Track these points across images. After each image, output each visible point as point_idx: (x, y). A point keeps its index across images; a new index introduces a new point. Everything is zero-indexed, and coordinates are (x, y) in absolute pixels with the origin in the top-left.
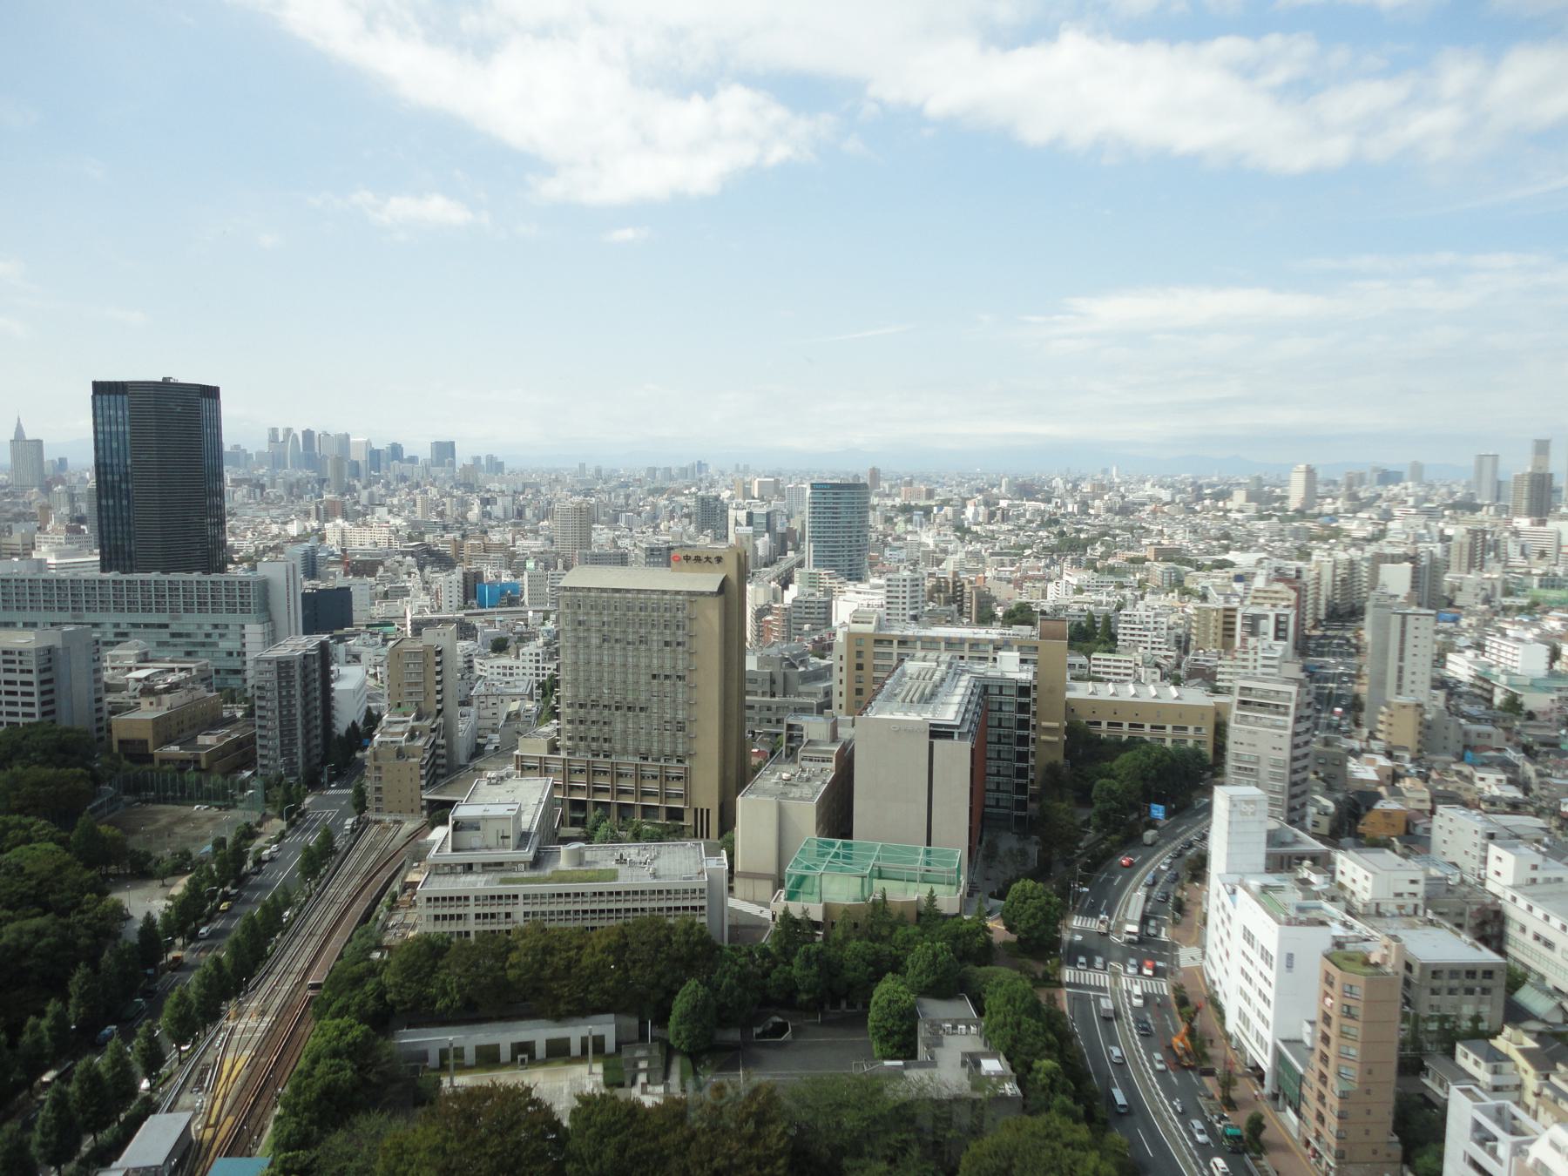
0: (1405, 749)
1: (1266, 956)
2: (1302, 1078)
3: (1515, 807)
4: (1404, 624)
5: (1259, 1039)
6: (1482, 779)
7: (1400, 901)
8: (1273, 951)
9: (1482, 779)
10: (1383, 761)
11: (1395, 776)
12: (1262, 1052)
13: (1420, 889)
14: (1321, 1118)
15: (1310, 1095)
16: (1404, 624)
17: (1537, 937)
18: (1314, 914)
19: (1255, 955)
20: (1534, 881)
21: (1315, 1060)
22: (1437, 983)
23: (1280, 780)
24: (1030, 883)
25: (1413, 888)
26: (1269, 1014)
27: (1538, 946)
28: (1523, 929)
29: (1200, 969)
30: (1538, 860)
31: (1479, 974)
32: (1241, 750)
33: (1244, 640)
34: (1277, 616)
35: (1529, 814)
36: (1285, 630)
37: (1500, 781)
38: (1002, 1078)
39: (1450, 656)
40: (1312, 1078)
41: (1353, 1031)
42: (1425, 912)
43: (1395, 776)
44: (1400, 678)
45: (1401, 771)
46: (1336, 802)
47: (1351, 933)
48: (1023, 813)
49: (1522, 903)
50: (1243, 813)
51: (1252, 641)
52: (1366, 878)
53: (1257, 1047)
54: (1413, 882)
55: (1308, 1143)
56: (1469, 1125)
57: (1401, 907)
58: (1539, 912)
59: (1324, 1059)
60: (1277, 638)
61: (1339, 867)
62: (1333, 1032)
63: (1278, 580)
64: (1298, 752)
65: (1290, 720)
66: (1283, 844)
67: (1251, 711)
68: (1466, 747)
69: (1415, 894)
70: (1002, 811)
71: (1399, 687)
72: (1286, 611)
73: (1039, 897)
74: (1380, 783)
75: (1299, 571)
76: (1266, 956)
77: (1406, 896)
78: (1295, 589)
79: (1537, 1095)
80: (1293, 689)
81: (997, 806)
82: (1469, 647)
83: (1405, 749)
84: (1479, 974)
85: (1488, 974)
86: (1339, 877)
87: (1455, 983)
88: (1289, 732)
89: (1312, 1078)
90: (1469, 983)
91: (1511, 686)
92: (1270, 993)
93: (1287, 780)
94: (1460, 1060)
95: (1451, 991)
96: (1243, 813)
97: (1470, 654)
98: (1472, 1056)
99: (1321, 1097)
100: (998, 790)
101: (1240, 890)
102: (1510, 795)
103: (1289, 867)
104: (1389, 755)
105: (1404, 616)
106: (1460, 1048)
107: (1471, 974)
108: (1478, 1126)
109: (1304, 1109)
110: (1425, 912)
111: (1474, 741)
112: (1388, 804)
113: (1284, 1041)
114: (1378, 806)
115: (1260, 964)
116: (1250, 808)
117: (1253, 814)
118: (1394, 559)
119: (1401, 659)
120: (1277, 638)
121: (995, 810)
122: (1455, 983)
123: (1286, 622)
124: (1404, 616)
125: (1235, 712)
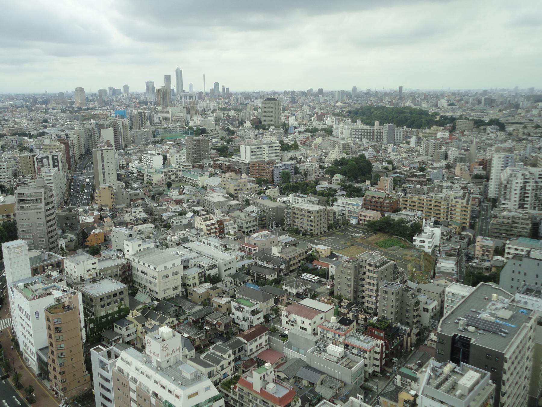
0: (107, 205)
1: (27, 316)
2: (47, 363)
3: (145, 221)
4: (102, 154)
5: (31, 352)
6: (135, 212)
7: (89, 273)
8: (29, 313)
9: (135, 212)
10: (96, 213)
11: (102, 218)
12: (33, 357)
15: (50, 369)
16: (102, 154)
17: (142, 272)
18: (48, 292)
19: (24, 317)
20: (140, 250)
21: (50, 354)
22: (102, 303)
23: (42, 232)
26: (32, 340)
27: (143, 275)
28: (138, 270)
30: (140, 242)
31: (118, 294)
32: (25, 223)
33: (39, 169)
34: (53, 157)
35: (149, 222)
36: (58, 162)
37: (140, 212)
39: (130, 164)
40: (50, 362)
43: (102, 218)
44: (104, 177)
45: (104, 215)
47: (66, 293)
49: (136, 261)
51: (42, 169)
52: (75, 267)
53: (31, 355)
54: (93, 264)
55: (53, 390)
56: (98, 362)
57: (90, 275)
58: (141, 263)
59: (52, 353)
60: (54, 166)
61: (65, 265)
62: (53, 341)
63: (57, 140)
64: (49, 218)
65: (43, 204)
66: (44, 261)
67: (25, 203)
68: (131, 200)
69: (95, 268)
71: (104, 180)
72: (57, 154)
74: (95, 222)
75: (67, 135)
76: (27, 316)
77: (92, 270)
78: (65, 143)
79: (141, 333)
80: (43, 191)
82: (137, 159)
83: (107, 205)
84: (118, 294)
85: (121, 293)
86: (66, 270)
87: (109, 300)
88: (43, 210)
89: (50, 362)
90: (115, 299)
91: (149, 173)
92: (31, 331)
93: (46, 231)
94: (115, 329)
95: (109, 304)
96: (16, 253)
97: (137, 162)
98: (119, 327)
99: (54, 369)
101: (14, 289)
102: (143, 217)
103: (44, 271)
104: (100, 210)
105: (102, 151)
106: (115, 324)
107: (115, 295)
108: (101, 362)
111: (134, 197)
112: (98, 231)
113: (40, 350)
114: (92, 233)
115: (26, 319)
116: (19, 250)
117: (21, 252)
118: (108, 126)
119: (103, 169)
120: (54, 166)
122: (109, 300)
123: (57, 159)
124: (102, 151)
125: (18, 206)
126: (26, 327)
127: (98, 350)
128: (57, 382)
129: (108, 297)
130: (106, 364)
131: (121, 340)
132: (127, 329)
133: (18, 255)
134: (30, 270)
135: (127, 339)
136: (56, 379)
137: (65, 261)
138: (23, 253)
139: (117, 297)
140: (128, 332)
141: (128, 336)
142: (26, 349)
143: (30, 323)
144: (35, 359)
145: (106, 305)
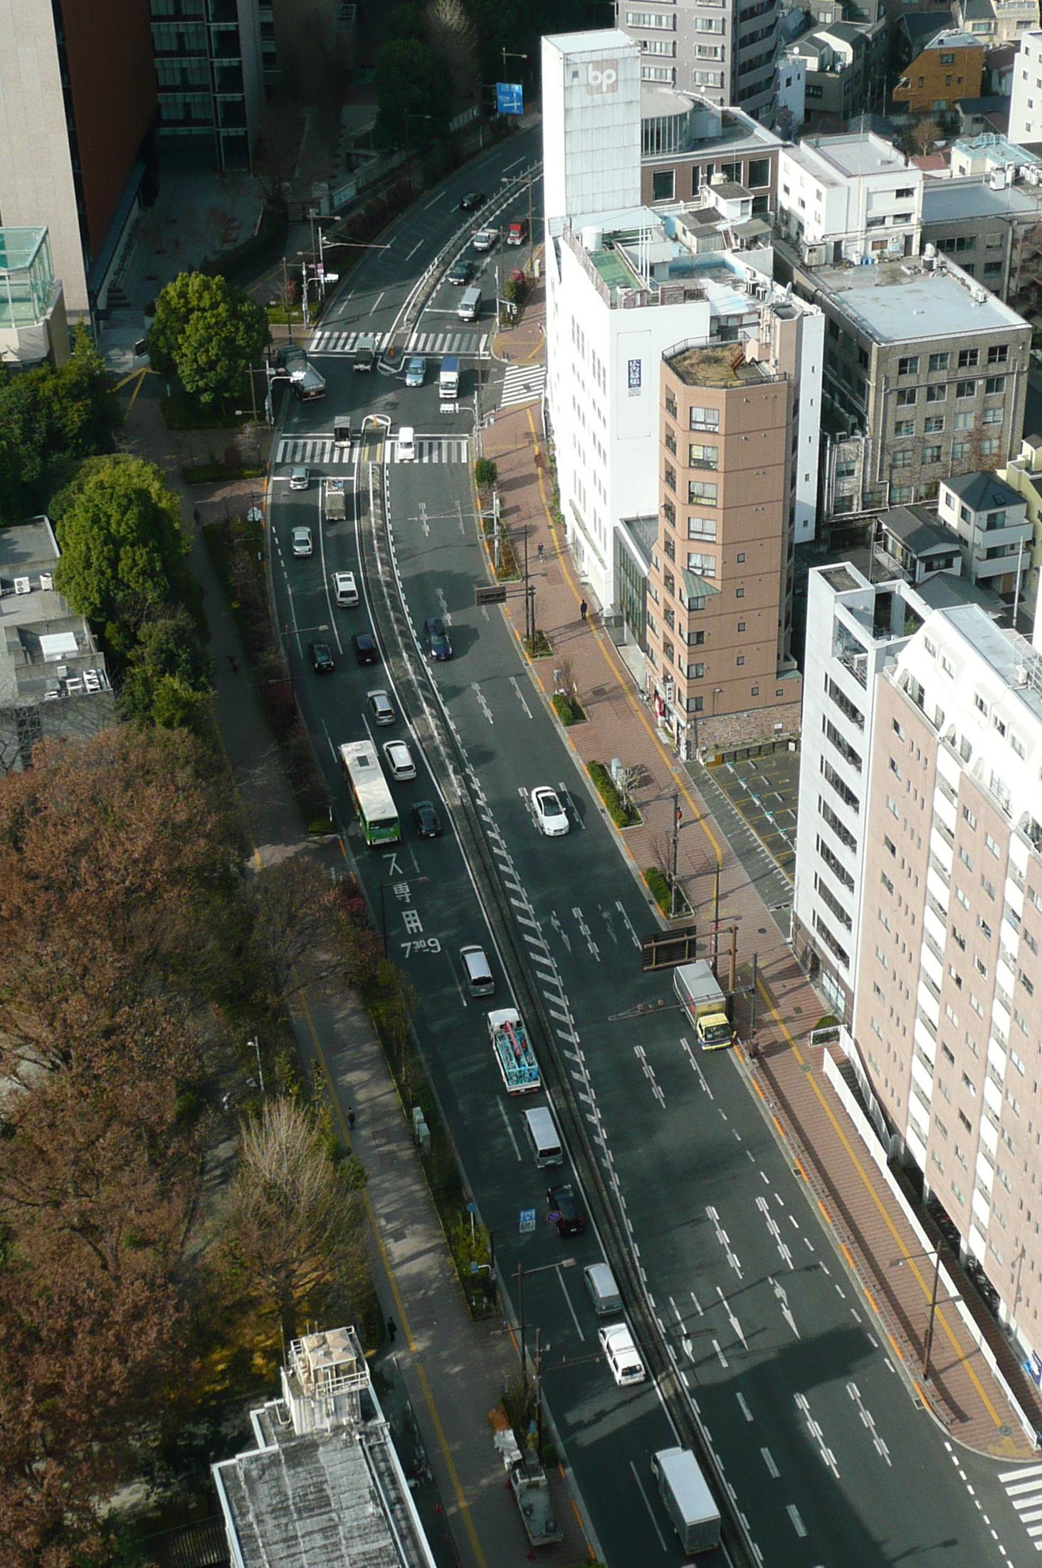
1: (599, 371)
7: (877, 231)
13: (914, 205)
14: (668, 647)
15: (655, 611)
18: (688, 284)
19: (586, 370)
22: (908, 381)
24: (195, 281)
25: (904, 205)
29: (541, 411)
31: (982, 356)
38: (73, 665)
41: (710, 491)
42: (922, 250)
46: (858, 43)
48: (240, 131)
50: (591, 89)
52: (819, 195)
54: (901, 193)
56: (830, 630)
61: (782, 180)
66: (701, 143)
69: (907, 217)
70: (196, 130)
73: (214, 306)
81: (188, 121)
84: (982, 356)
85: (998, 353)
87: (940, 377)
89: (656, 583)
90: (963, 373)
92: (604, 437)
96: (592, 90)
99: (668, 614)
100: (186, 87)
103: (695, 191)
107: (967, 357)
108: (842, 632)
109: (649, 639)
110: (922, 250)
113: (629, 523)
114: (933, 44)
115: (592, 383)
117: (613, 88)
121: (182, 131)
122: (940, 377)
126: (591, 415)
127: (837, 581)
128: (674, 672)
129: (936, 360)
130: (859, 649)
131: (957, 562)
132: (992, 524)
133: (598, 97)
134: (639, 171)
135: (986, 569)
136: (671, 657)
137: (783, 157)
138: (621, 95)
139: (975, 371)
140: (997, 538)
141: (993, 553)
142: (579, 507)
143: (605, 404)
144: (609, 556)
145: (921, 394)
